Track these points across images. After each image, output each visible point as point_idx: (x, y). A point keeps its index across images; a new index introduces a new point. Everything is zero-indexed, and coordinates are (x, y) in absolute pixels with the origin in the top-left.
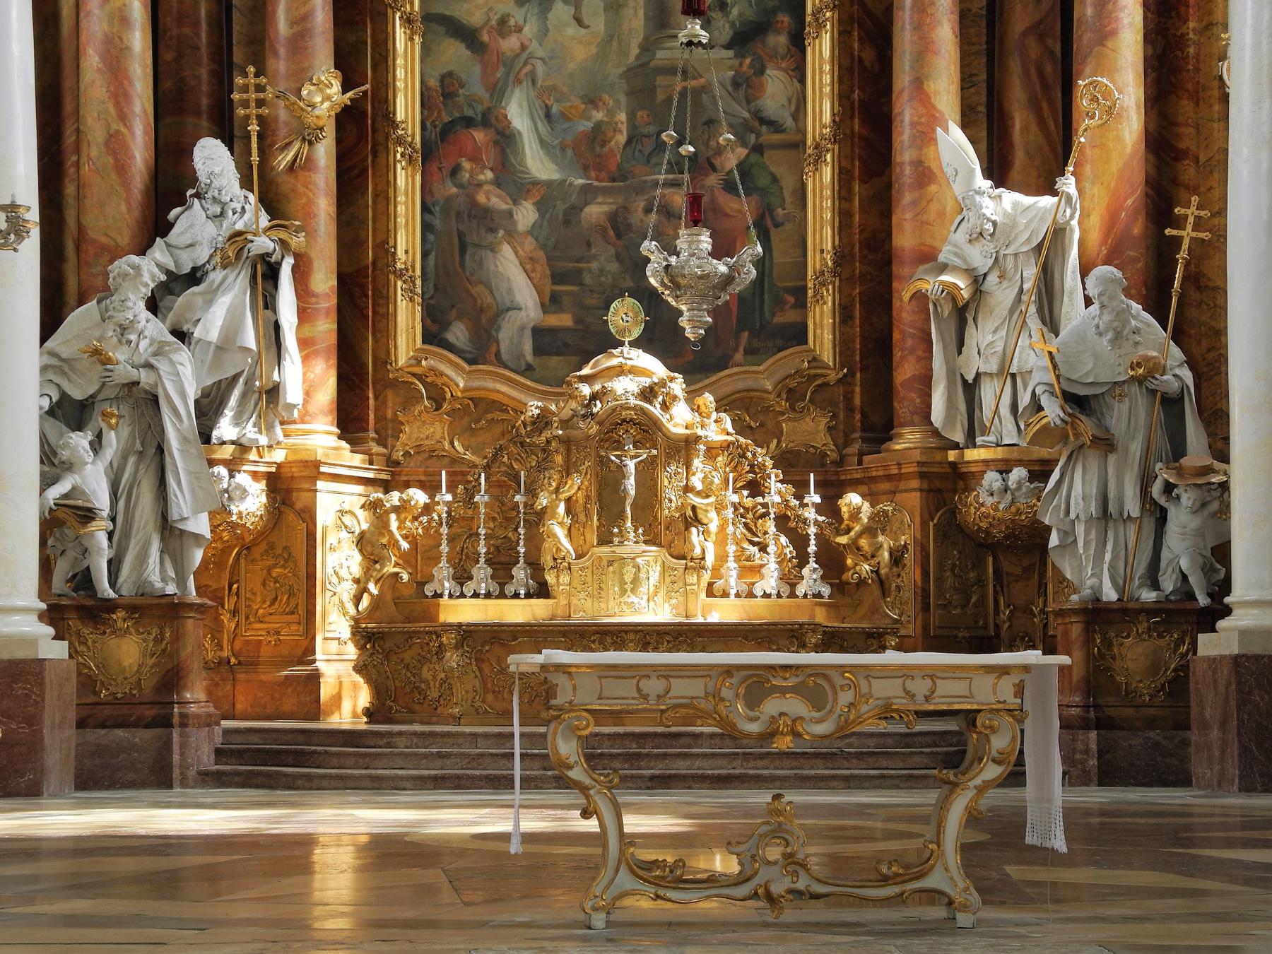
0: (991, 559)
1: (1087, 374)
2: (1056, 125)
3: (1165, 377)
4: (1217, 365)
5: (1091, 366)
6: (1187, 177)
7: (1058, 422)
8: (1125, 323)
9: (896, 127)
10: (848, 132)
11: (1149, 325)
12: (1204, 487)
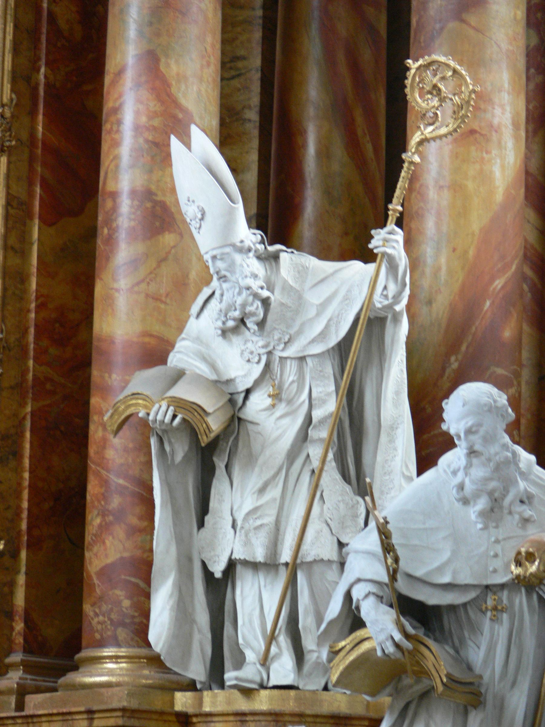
1: (440, 569)
2: (376, 150)
5: (446, 555)
7: (390, 649)
9: (109, 132)
10: (25, 136)
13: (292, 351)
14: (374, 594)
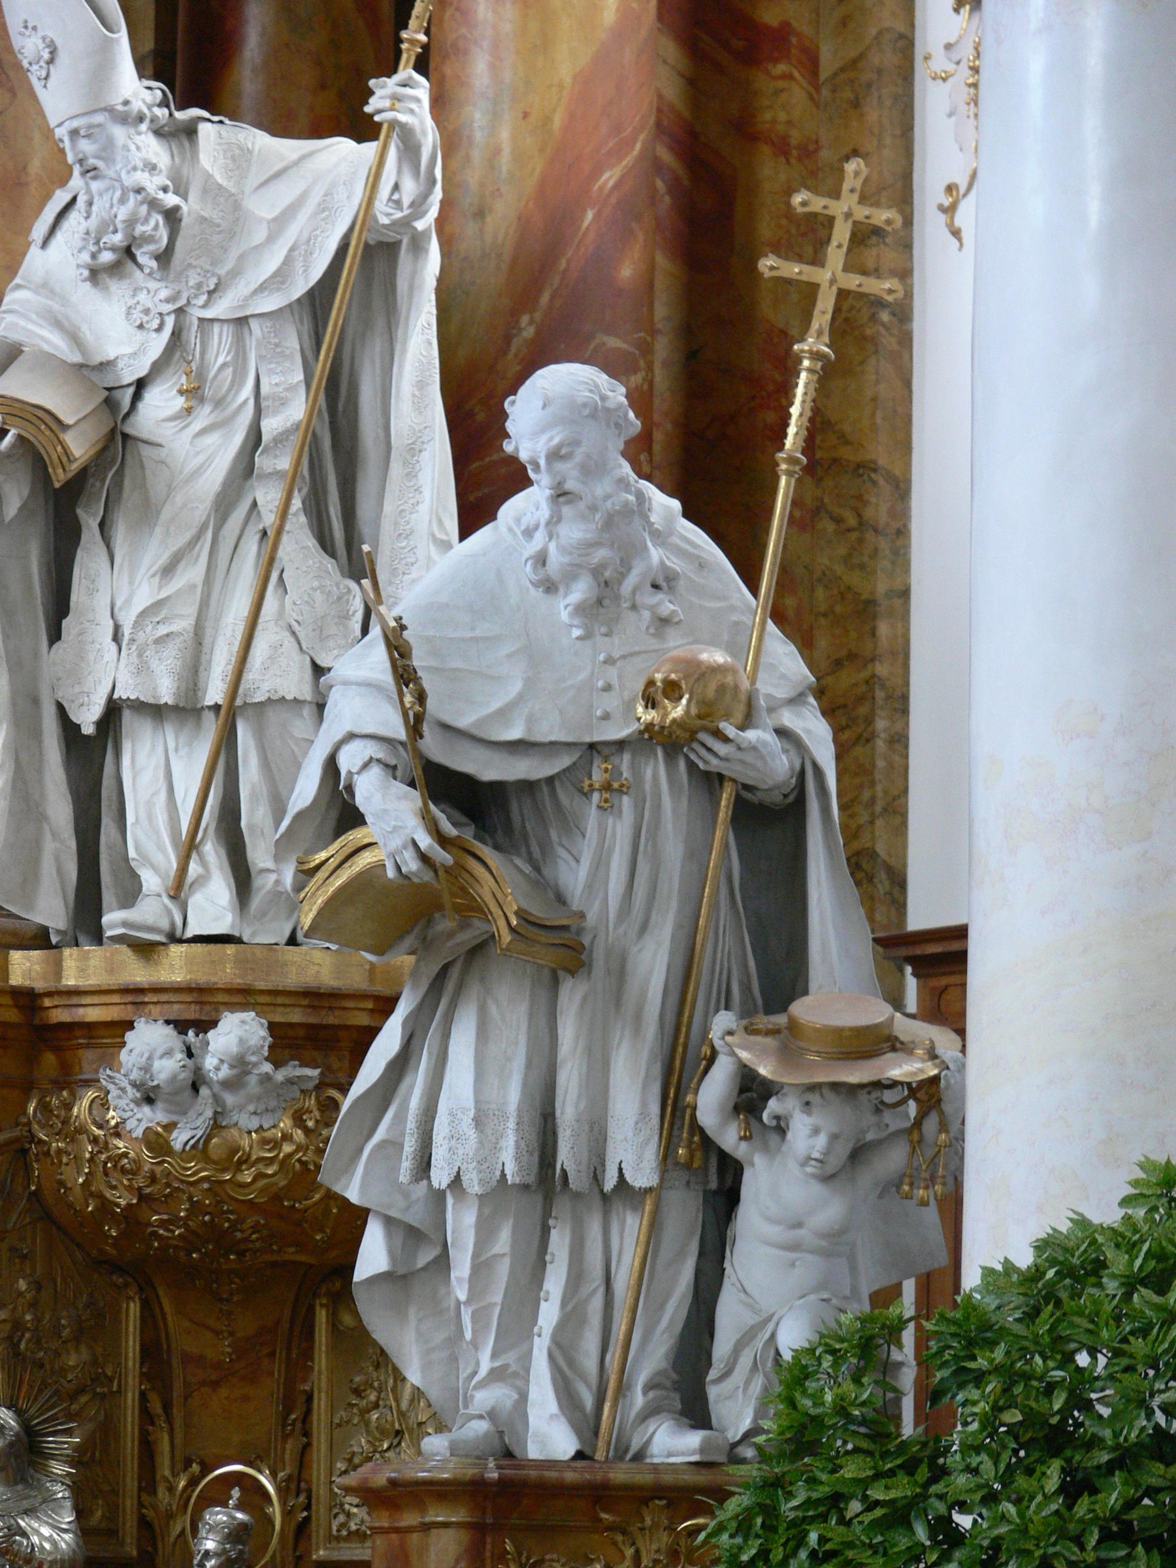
0: (134, 1309)
1: (503, 714)
3: (751, 735)
4: (862, 710)
5: (515, 688)
6: (782, 116)
8: (629, 553)
11: (702, 565)
12: (863, 1096)
13: (221, 308)
14: (379, 761)
